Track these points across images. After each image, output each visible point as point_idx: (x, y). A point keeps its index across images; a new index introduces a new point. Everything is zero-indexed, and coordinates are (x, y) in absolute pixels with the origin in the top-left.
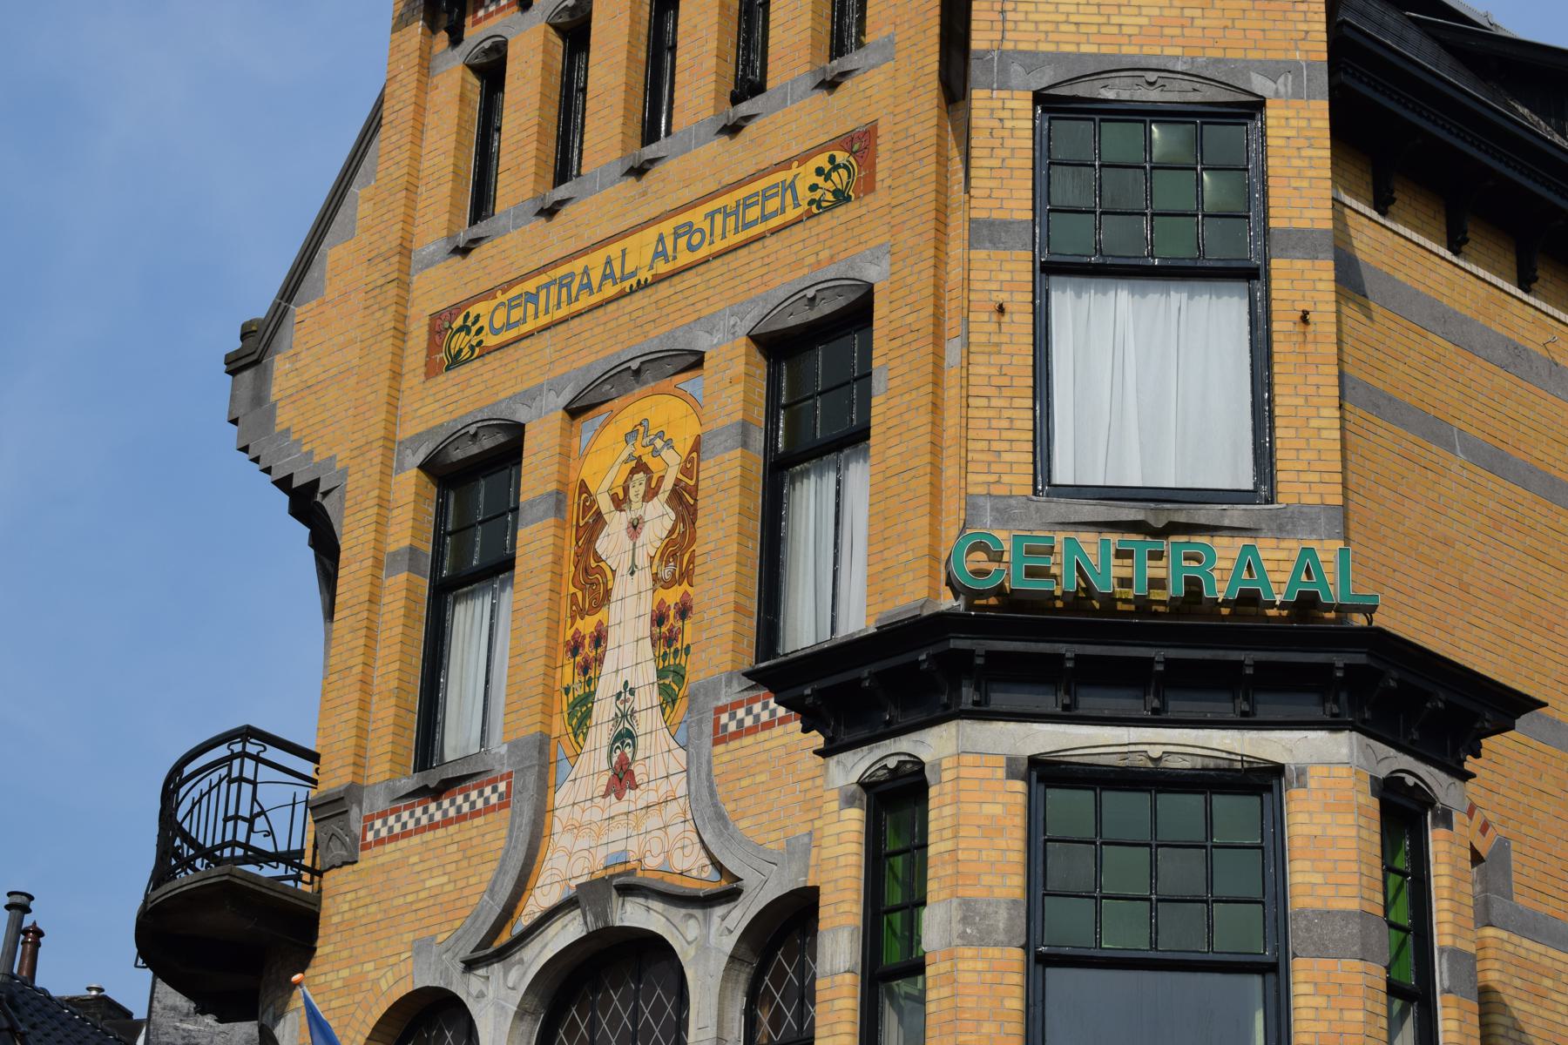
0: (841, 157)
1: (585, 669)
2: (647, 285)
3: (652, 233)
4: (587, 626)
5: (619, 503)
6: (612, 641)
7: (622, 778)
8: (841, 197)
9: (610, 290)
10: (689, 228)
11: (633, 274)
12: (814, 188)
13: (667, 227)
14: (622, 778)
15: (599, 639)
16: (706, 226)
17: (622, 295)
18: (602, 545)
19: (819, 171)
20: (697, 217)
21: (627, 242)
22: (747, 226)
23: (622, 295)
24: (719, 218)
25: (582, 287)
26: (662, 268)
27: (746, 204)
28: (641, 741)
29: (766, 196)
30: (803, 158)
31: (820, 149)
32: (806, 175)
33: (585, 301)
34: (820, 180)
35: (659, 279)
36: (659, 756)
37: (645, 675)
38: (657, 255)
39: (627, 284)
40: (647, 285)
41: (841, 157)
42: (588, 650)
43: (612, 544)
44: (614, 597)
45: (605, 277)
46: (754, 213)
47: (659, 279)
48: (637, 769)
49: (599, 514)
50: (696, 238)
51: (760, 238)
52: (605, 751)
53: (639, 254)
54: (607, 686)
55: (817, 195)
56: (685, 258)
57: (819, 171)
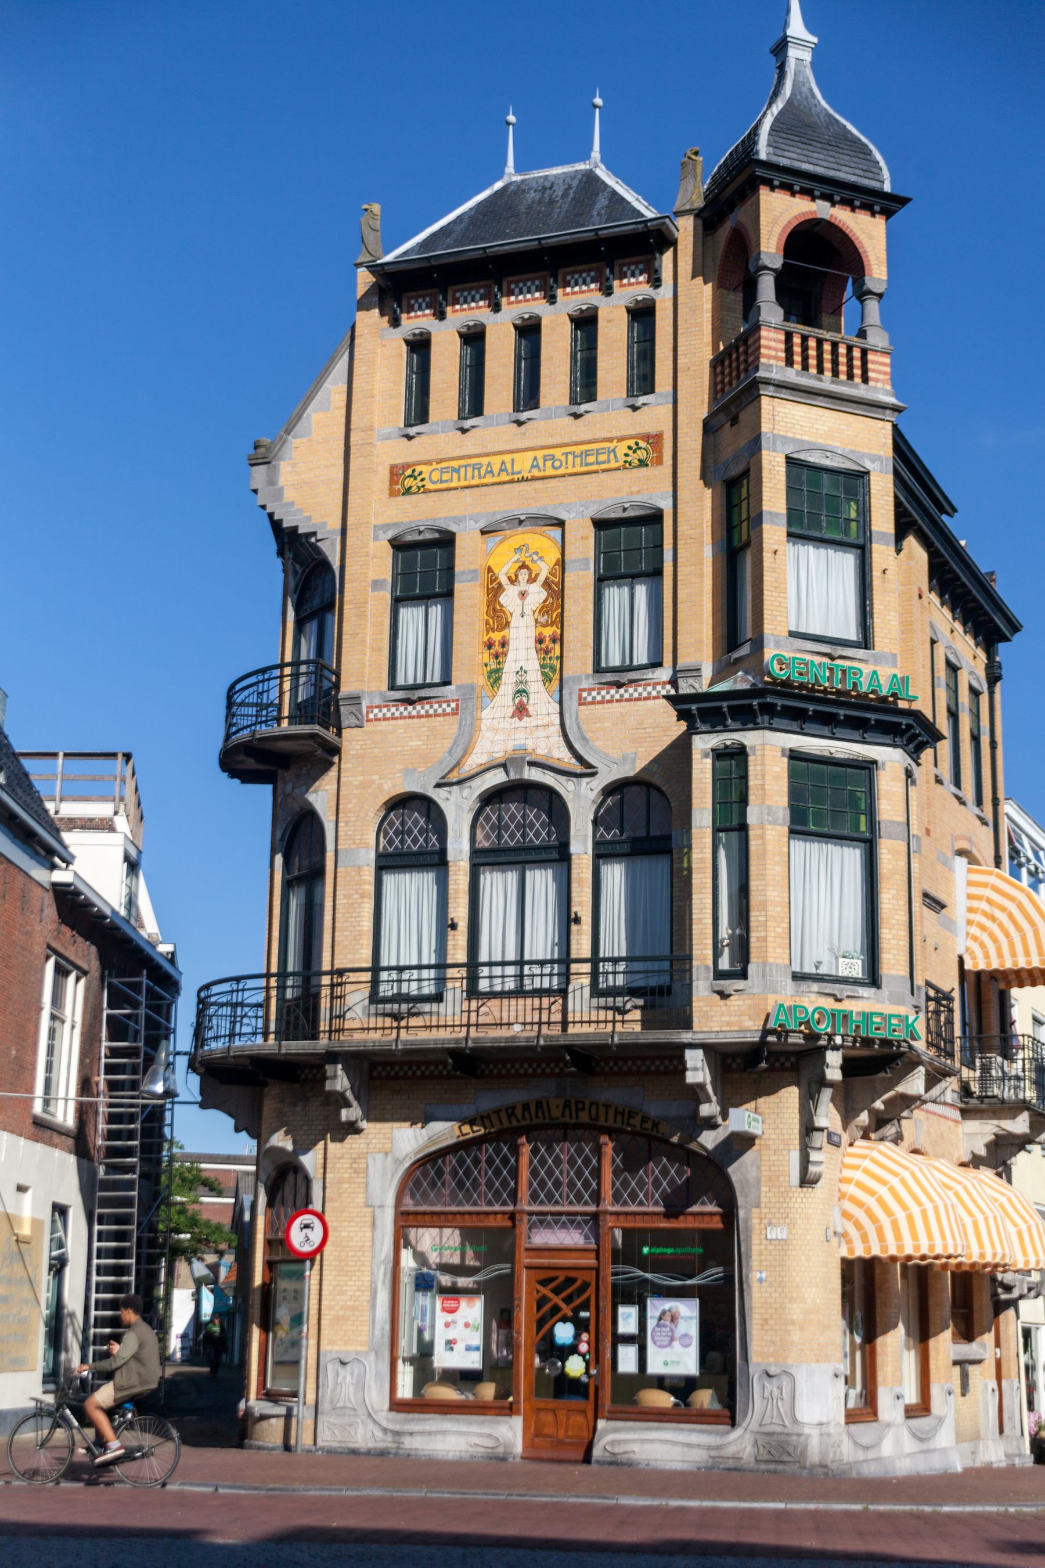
0: (642, 444)
1: (497, 656)
2: (527, 480)
3: (530, 455)
4: (497, 636)
5: (513, 581)
6: (512, 645)
7: (521, 711)
8: (643, 463)
9: (504, 477)
10: (553, 458)
11: (519, 473)
12: (626, 455)
13: (539, 454)
14: (521, 711)
15: (504, 644)
16: (563, 458)
17: (512, 482)
18: (503, 599)
19: (630, 448)
20: (558, 453)
21: (513, 456)
22: (587, 464)
23: (512, 482)
24: (570, 457)
25: (487, 472)
26: (536, 473)
27: (587, 453)
28: (532, 696)
29: (598, 452)
30: (621, 439)
31: (631, 437)
32: (622, 448)
33: (489, 479)
34: (630, 452)
35: (534, 479)
36: (543, 703)
37: (533, 665)
38: (533, 466)
39: (516, 477)
40: (527, 480)
41: (642, 444)
42: (497, 648)
43: (509, 599)
44: (512, 625)
45: (501, 470)
46: (591, 459)
47: (534, 479)
48: (531, 709)
49: (500, 585)
50: (557, 464)
51: (596, 472)
52: (510, 697)
53: (523, 463)
54: (510, 667)
55: (629, 459)
56: (550, 472)
57: (630, 448)
